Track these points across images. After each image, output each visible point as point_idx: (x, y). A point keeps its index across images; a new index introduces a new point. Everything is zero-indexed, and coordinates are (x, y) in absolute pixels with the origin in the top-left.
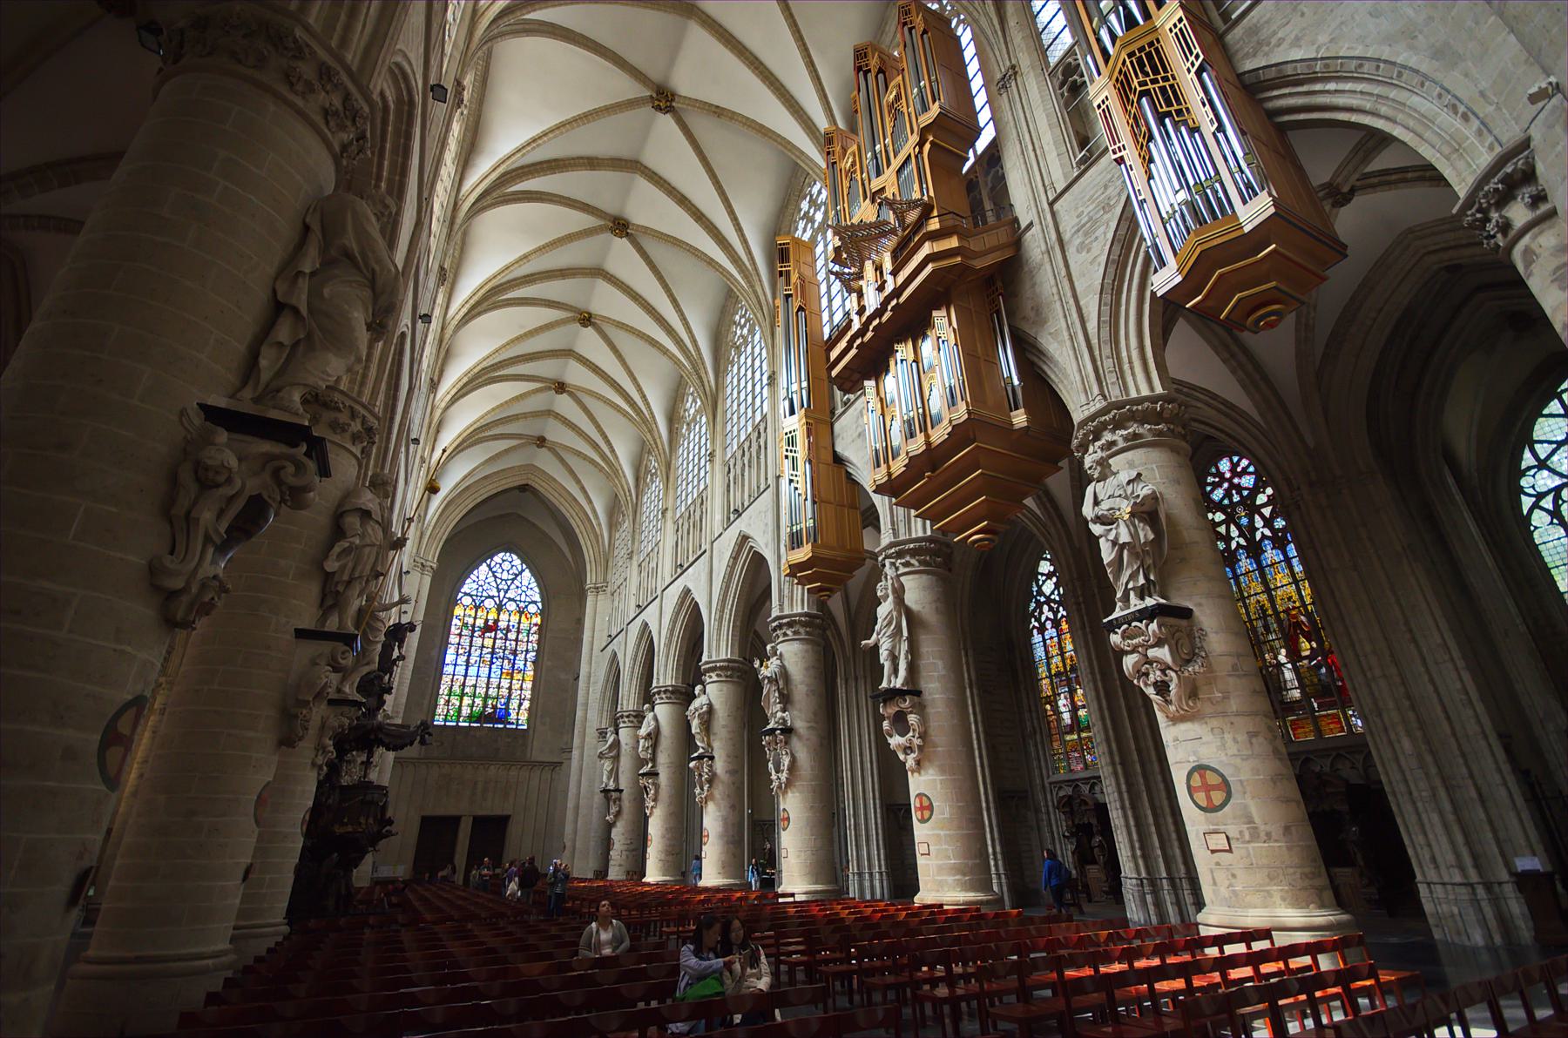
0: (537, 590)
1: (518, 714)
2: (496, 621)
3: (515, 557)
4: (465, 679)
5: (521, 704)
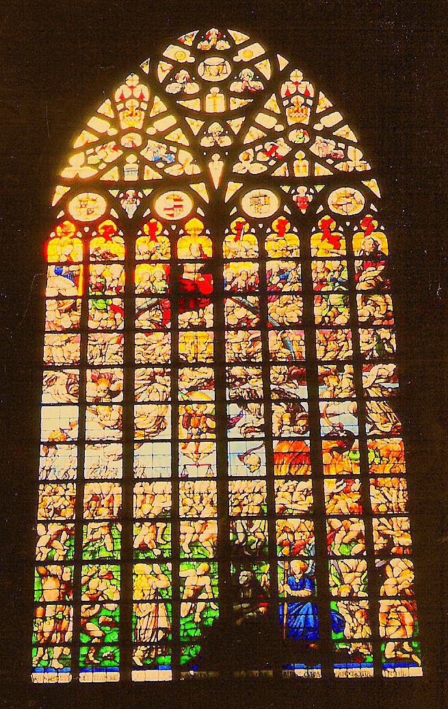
0: (346, 132)
1: (372, 617)
2: (214, 264)
3: (239, 37)
4: (128, 496)
5: (375, 578)
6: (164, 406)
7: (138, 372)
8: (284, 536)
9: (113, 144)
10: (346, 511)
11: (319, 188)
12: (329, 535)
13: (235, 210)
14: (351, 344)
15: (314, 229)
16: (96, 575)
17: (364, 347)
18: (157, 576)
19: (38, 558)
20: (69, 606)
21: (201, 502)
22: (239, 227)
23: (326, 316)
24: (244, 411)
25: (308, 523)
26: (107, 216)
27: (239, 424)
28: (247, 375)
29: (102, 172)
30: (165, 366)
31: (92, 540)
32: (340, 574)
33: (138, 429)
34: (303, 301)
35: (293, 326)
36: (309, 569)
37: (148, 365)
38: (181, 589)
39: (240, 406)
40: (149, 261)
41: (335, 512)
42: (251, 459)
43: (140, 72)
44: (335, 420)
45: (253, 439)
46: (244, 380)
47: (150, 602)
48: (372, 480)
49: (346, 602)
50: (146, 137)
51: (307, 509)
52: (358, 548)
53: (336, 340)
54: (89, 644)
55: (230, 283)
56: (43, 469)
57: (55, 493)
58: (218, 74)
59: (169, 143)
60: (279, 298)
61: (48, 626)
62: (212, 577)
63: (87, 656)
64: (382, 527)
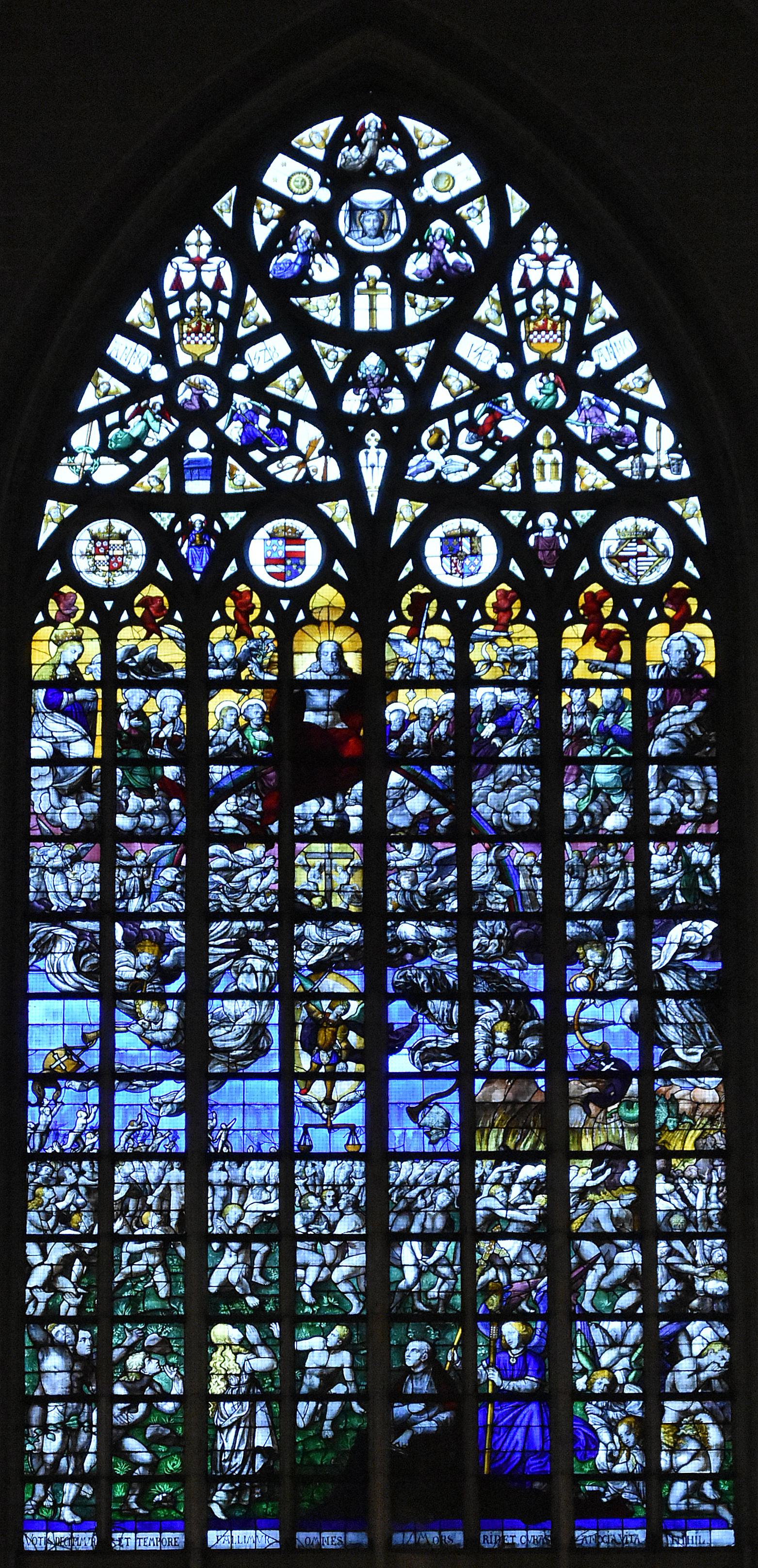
6: (265, 1003)
7: (217, 928)
8: (491, 1273)
9: (158, 400)
10: (608, 1227)
11: (583, 516)
12: (575, 1274)
13: (409, 566)
14: (631, 876)
15: (569, 615)
16: (139, 1345)
17: (659, 882)
18: (251, 1349)
19: (30, 1310)
20: (90, 1405)
21: (336, 1202)
22: (419, 603)
23: (587, 811)
24: (420, 1016)
25: (536, 1248)
26: (148, 575)
27: (411, 1042)
28: (427, 939)
29: (138, 471)
30: (266, 916)
31: (131, 1276)
32: (593, 1350)
33: (216, 1050)
34: (541, 778)
35: (521, 834)
36: (536, 1339)
37: (236, 915)
38: (298, 1373)
39: (412, 1005)
40: (234, 684)
41: (589, 1229)
42: (434, 1117)
43: (213, 225)
44: (595, 1037)
45: (436, 1075)
46: (422, 951)
47: (240, 1398)
48: (660, 1163)
49: (601, 1404)
50: (227, 388)
51: (532, 1218)
52: (627, 1299)
53: (605, 865)
54: (128, 1479)
55: (397, 735)
56: (35, 1129)
57: (59, 1181)
58: (380, 233)
59: (277, 403)
60: (494, 771)
61: (51, 1445)
62: (353, 1355)
63: (124, 1500)
64: (671, 1260)
